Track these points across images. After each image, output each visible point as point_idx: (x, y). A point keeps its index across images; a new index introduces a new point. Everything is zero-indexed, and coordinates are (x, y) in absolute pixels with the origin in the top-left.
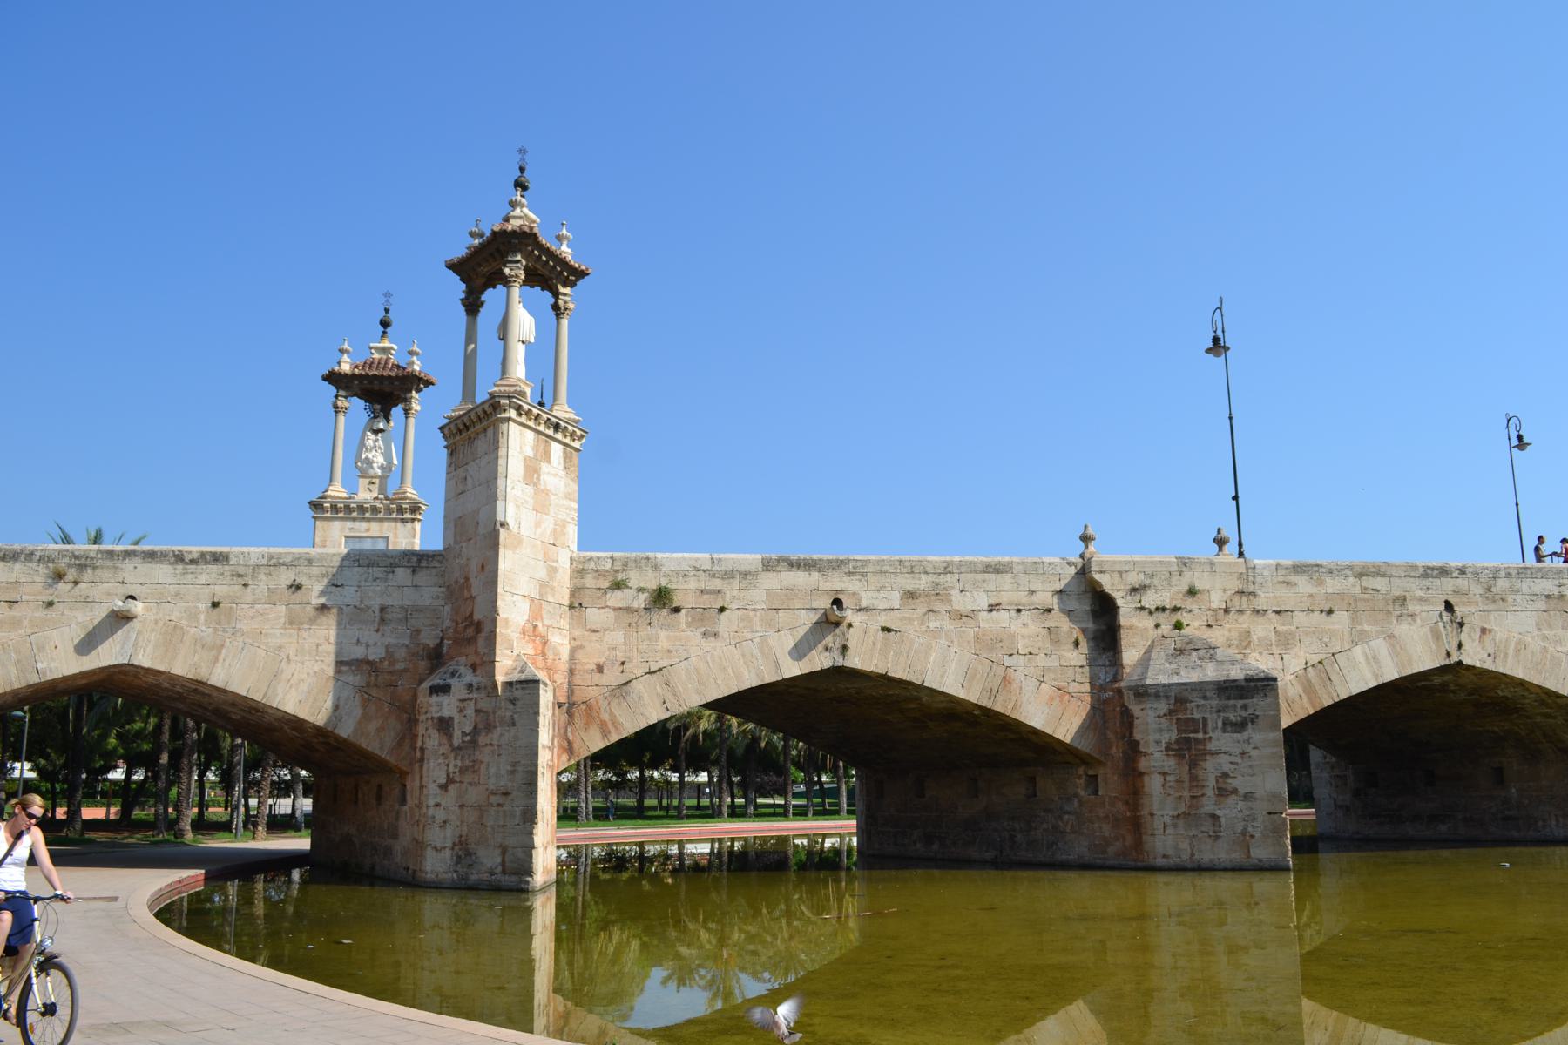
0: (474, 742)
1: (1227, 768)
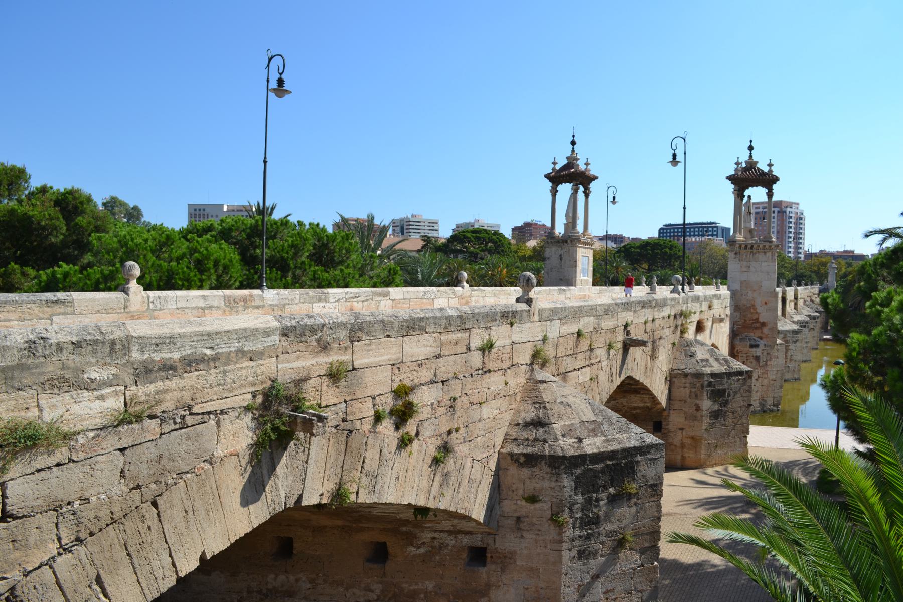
0: (766, 364)
1: (792, 353)
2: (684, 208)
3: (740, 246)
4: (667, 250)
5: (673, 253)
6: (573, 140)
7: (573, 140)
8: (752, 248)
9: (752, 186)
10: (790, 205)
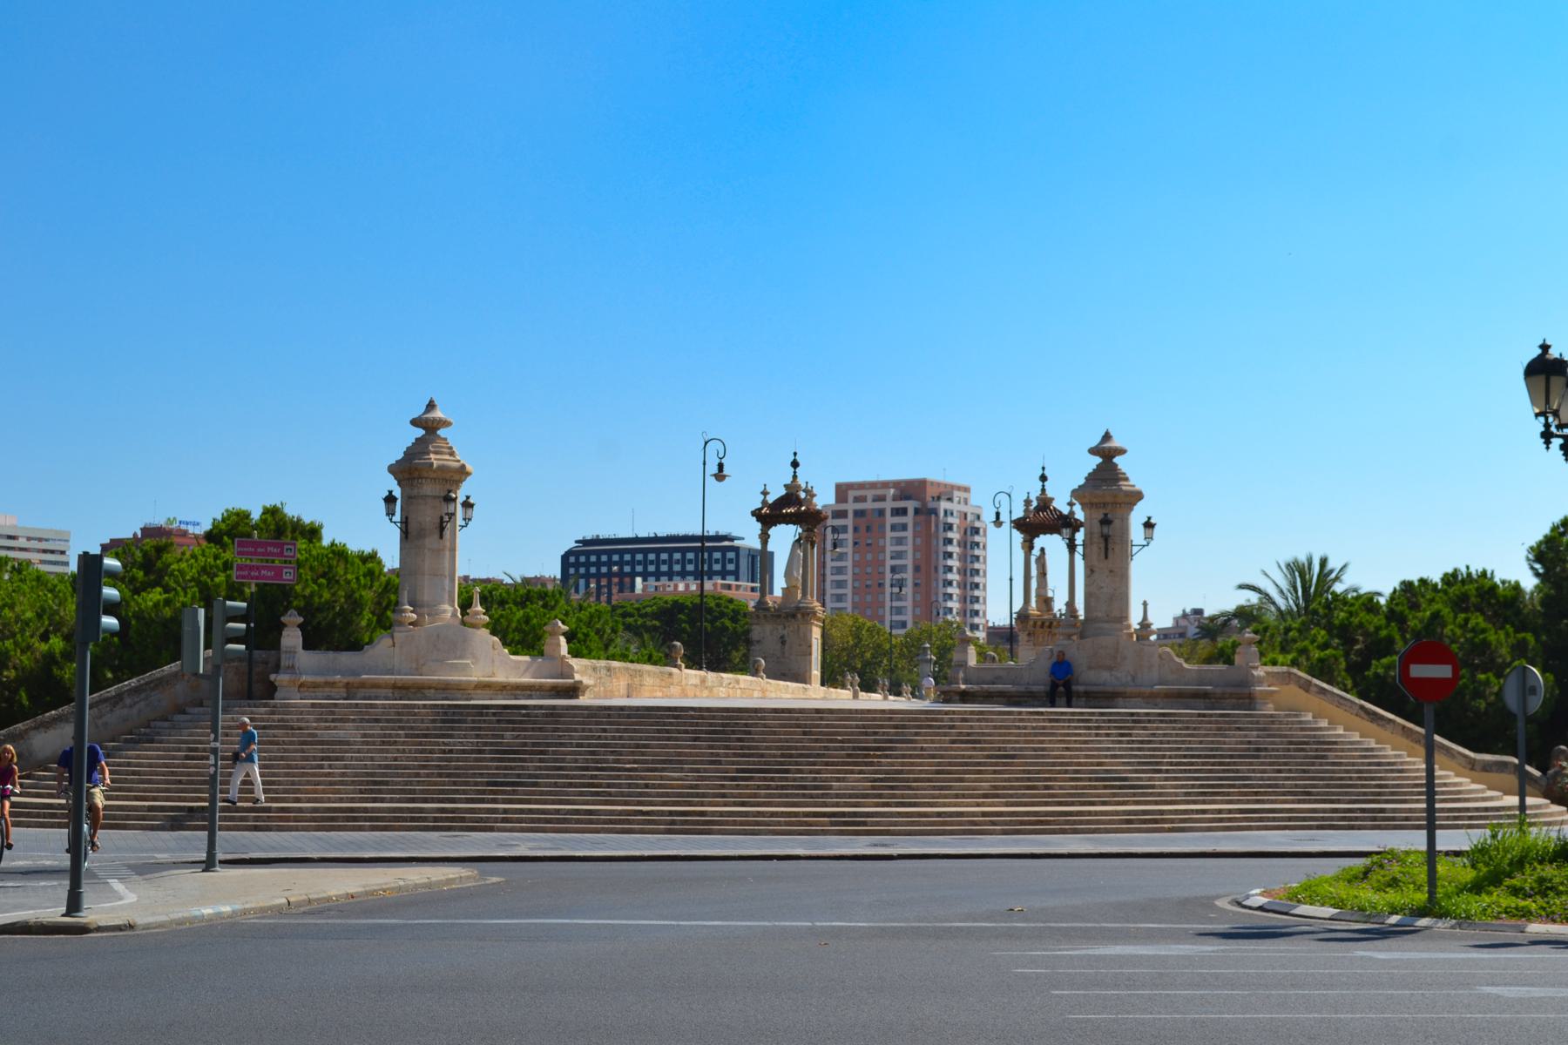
2: (1011, 580)
3: (1035, 624)
4: (728, 623)
5: (740, 630)
6: (795, 460)
7: (795, 460)
8: (1051, 624)
9: (1045, 534)
10: (947, 492)
